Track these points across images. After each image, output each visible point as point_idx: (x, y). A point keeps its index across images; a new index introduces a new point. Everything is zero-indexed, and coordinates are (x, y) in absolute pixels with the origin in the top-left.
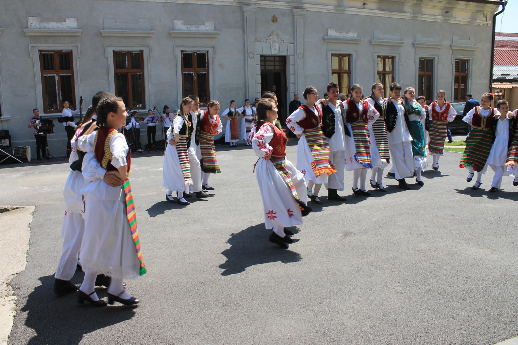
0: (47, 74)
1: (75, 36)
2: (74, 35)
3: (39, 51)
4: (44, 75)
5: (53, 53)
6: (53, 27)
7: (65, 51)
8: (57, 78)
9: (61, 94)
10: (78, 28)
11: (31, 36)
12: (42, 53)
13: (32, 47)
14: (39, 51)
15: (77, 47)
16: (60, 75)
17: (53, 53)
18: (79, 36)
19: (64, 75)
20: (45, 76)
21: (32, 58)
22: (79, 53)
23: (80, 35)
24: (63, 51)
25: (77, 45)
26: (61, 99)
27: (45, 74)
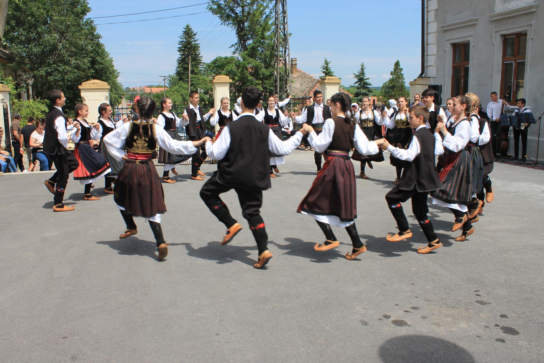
0: (507, 61)
1: (531, 13)
2: (528, 11)
3: (501, 35)
4: (505, 62)
5: (514, 36)
6: (513, 6)
7: (524, 33)
8: (514, 64)
9: (515, 83)
10: (535, 2)
11: (496, 21)
12: (506, 37)
13: (496, 32)
14: (504, 36)
15: (531, 25)
16: (518, 61)
17: (514, 36)
18: (535, 12)
19: (520, 61)
20: (506, 63)
21: (494, 44)
22: (533, 33)
23: (534, 10)
24: (522, 32)
25: (530, 23)
26: (515, 89)
27: (506, 61)
